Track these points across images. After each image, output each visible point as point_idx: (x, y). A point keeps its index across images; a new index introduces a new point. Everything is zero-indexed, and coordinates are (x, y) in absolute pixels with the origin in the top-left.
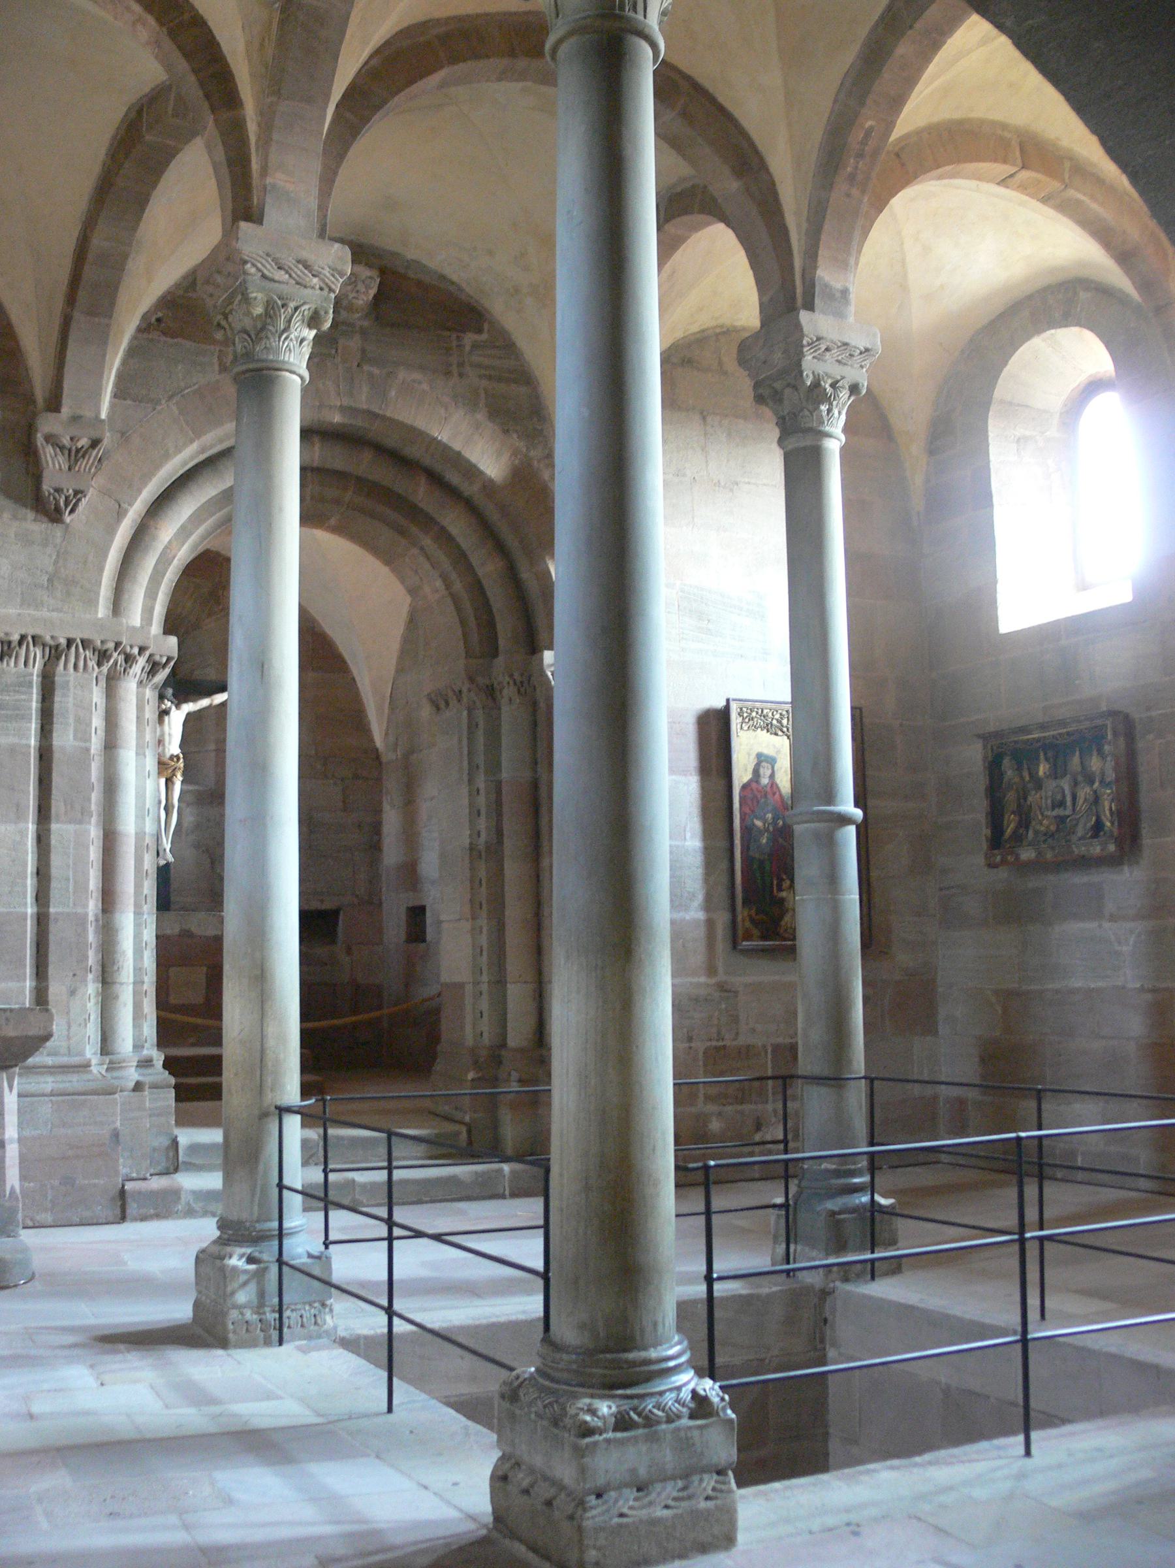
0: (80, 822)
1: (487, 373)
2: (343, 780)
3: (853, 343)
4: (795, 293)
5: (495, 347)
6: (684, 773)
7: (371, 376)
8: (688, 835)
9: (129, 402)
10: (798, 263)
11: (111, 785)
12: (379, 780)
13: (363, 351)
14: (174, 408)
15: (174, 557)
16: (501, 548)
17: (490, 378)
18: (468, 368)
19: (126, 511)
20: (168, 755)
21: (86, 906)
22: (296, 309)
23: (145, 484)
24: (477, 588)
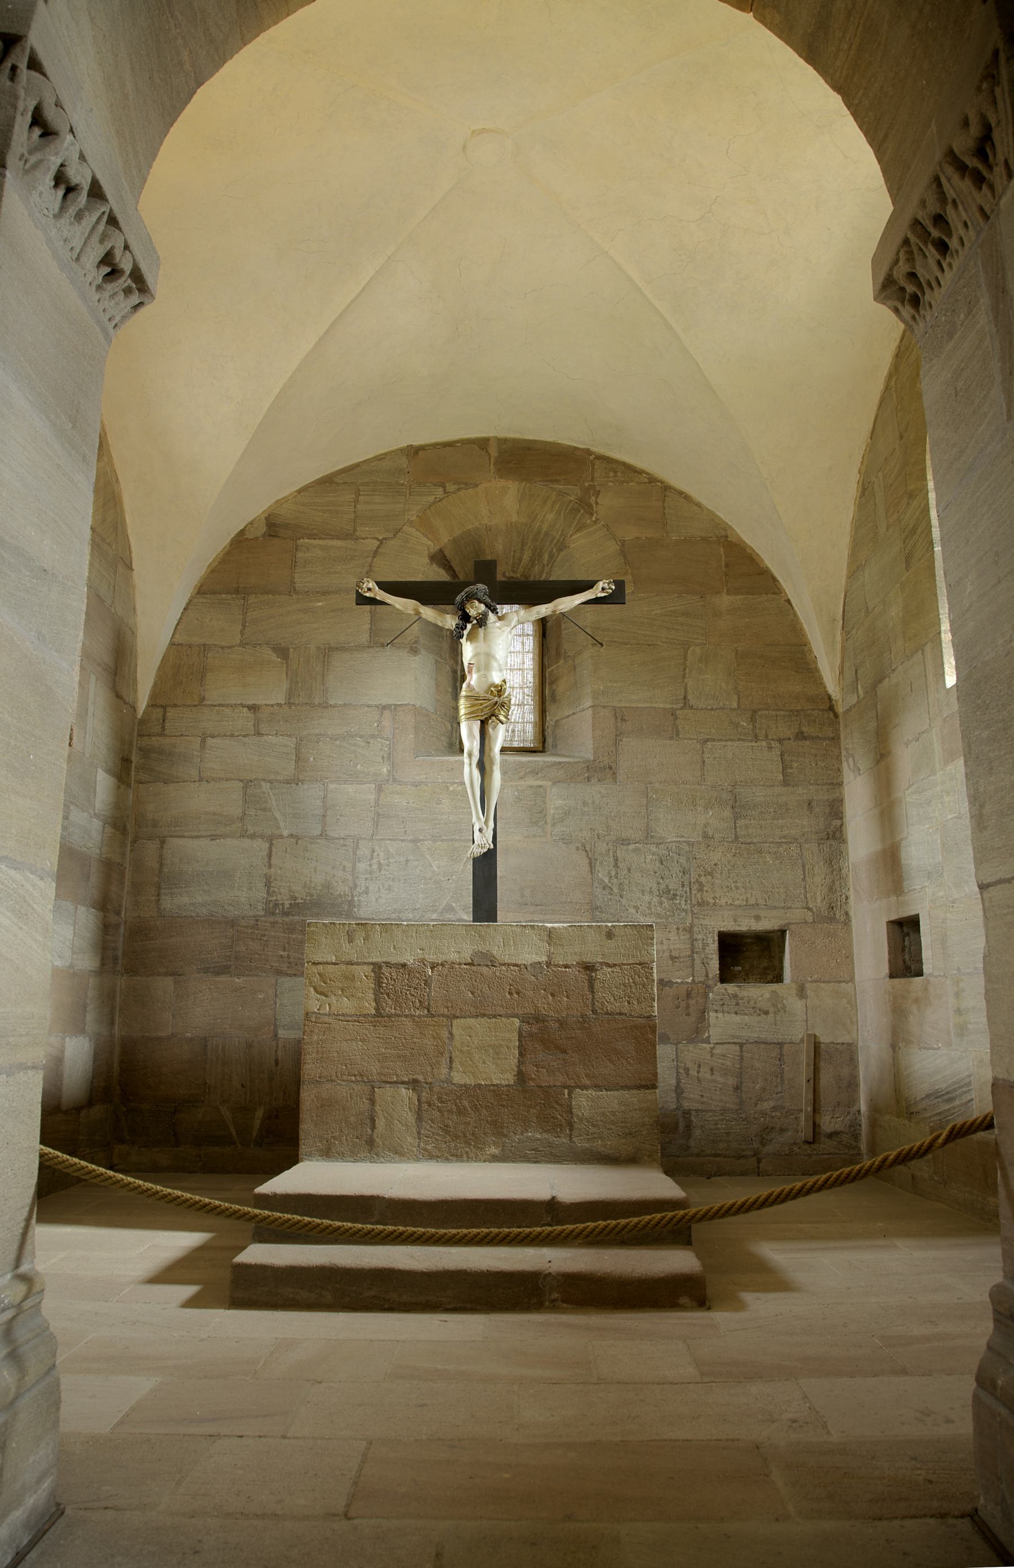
2: (780, 741)
12: (836, 739)
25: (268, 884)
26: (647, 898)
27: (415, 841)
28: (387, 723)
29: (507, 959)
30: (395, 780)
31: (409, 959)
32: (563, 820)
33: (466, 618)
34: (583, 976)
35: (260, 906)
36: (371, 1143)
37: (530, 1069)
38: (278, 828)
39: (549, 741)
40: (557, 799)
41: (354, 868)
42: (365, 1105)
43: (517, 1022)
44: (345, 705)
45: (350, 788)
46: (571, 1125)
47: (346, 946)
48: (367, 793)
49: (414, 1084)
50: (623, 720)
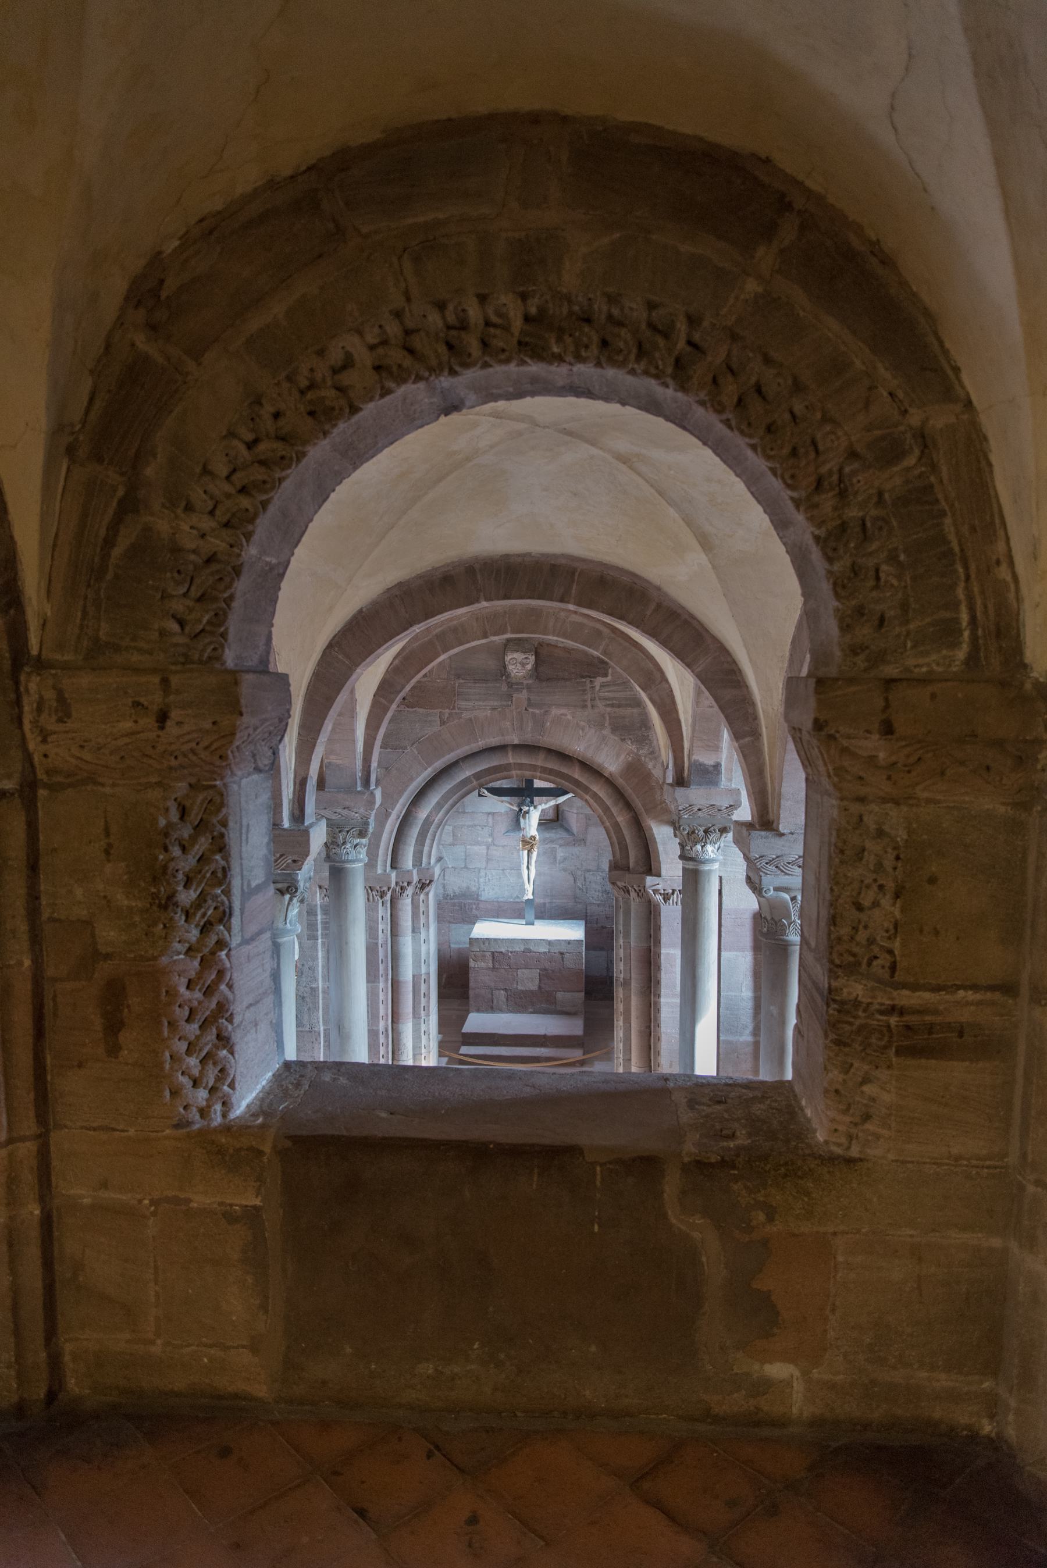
0: (374, 982)
1: (611, 703)
3: (717, 803)
4: (683, 767)
5: (615, 685)
6: (743, 950)
7: (533, 714)
8: (744, 989)
9: (389, 750)
10: (686, 745)
11: (395, 957)
13: (529, 699)
14: (415, 750)
15: (434, 820)
16: (628, 806)
17: (612, 706)
18: (598, 701)
19: (391, 813)
20: (529, 837)
21: (378, 1026)
22: (348, 832)
23: (401, 797)
24: (616, 826)
25: (444, 887)
26: (597, 893)
27: (503, 870)
28: (490, 820)
29: (535, 951)
30: (494, 845)
31: (503, 950)
32: (563, 862)
33: (521, 810)
34: (560, 956)
35: (441, 896)
36: (492, 1008)
37: (543, 986)
38: (447, 863)
39: (560, 817)
40: (561, 853)
41: (478, 881)
42: (490, 996)
43: (538, 970)
44: (472, 812)
45: (476, 848)
46: (556, 1003)
47: (482, 946)
48: (483, 850)
49: (505, 990)
50: (589, 819)
